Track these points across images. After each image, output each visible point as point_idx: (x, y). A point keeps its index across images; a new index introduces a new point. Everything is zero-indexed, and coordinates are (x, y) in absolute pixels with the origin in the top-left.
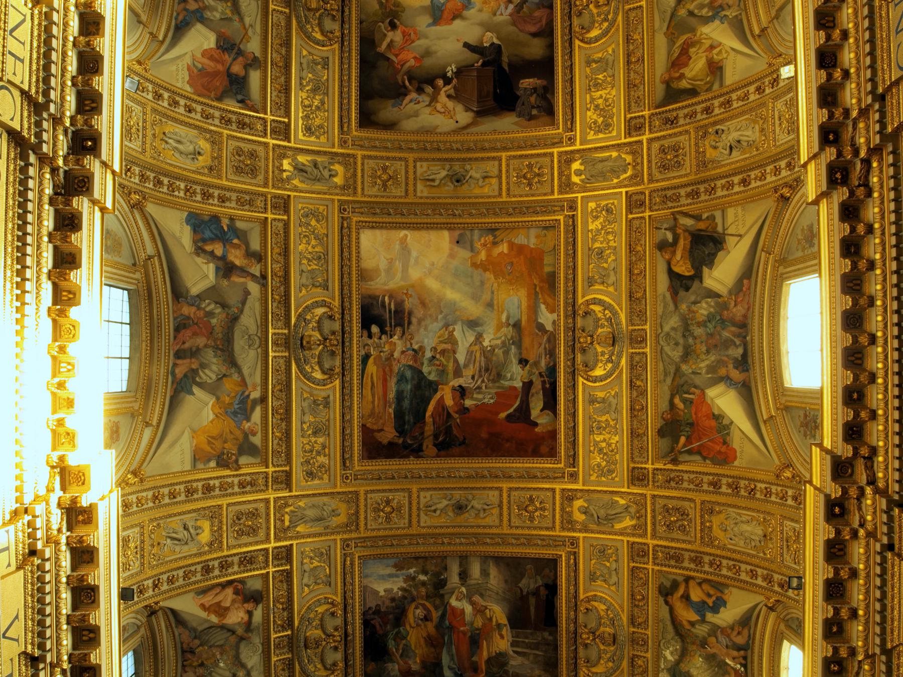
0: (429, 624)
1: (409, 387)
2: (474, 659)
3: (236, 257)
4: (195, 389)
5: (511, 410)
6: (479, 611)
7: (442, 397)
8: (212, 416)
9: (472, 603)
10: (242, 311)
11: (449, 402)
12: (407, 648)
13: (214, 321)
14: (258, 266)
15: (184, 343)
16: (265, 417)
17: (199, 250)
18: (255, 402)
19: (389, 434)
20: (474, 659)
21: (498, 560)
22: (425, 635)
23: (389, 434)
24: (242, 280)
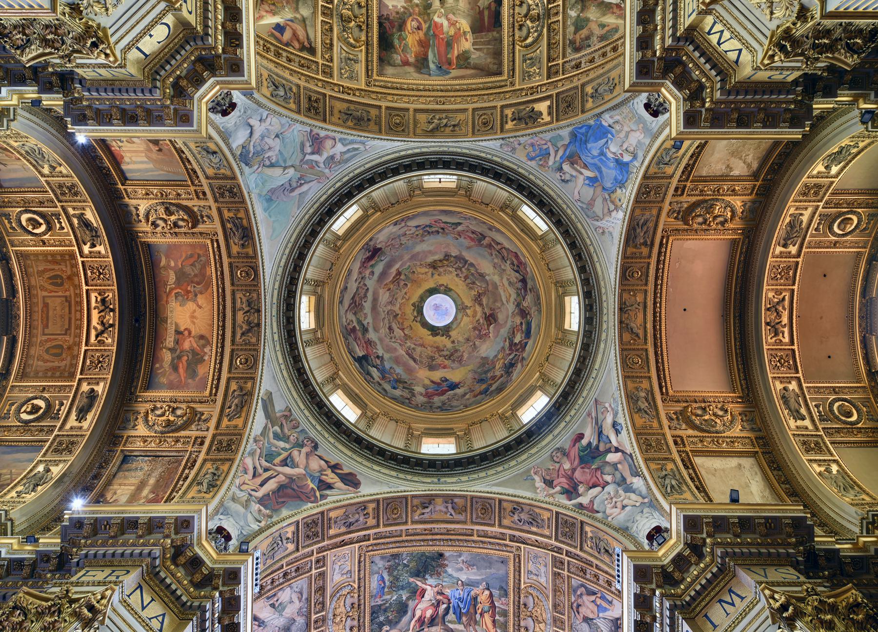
0: (420, 32)
2: (449, 56)
12: (406, 45)
20: (449, 56)
22: (418, 38)
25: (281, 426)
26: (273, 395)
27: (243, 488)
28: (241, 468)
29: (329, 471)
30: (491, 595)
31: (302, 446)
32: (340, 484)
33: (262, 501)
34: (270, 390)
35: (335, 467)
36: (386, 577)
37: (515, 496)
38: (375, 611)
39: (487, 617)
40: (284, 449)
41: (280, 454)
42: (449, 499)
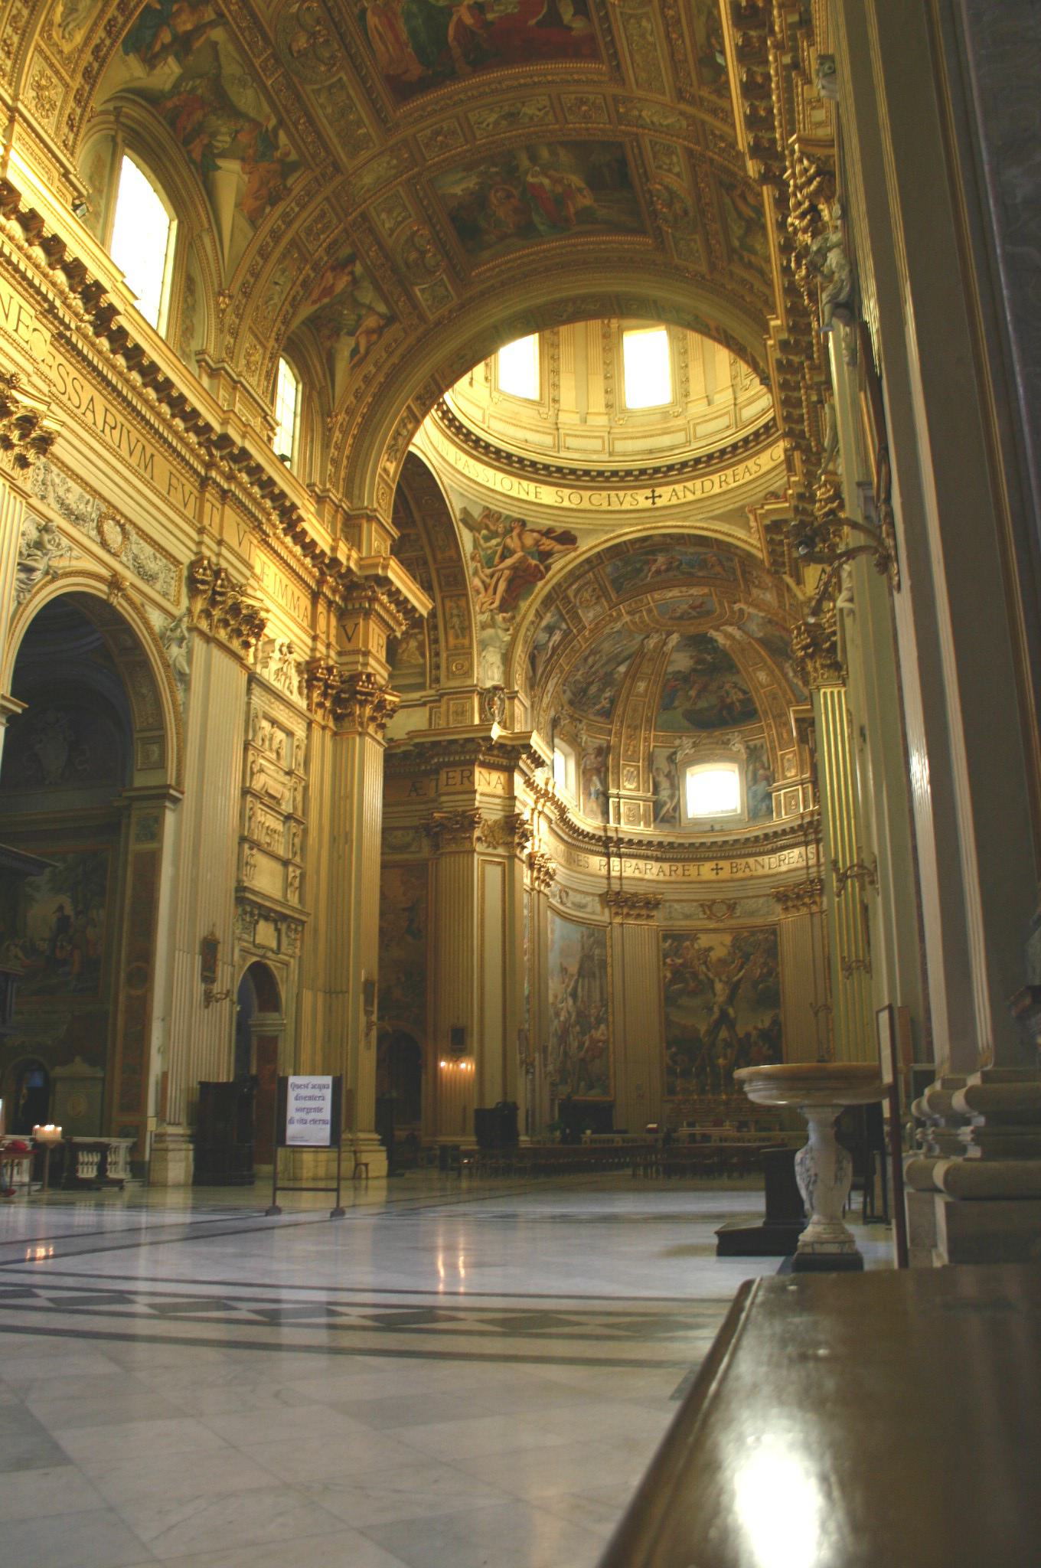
1: (420, 21)
3: (184, 23)
4: (220, 162)
5: (541, 16)
6: (555, 181)
7: (460, 20)
8: (246, 178)
9: (549, 177)
10: (220, 67)
11: (468, 20)
13: (199, 92)
14: (210, 8)
15: (185, 129)
16: (290, 135)
17: (151, 61)
18: (275, 131)
19: (416, 70)
21: (563, 144)
23: (416, 70)
24: (203, 39)
25: (487, 527)
26: (469, 509)
27: (483, 610)
28: (474, 593)
29: (544, 540)
30: (719, 560)
31: (512, 530)
32: (559, 547)
33: (502, 608)
34: (463, 506)
35: (548, 533)
36: (619, 563)
37: (729, 535)
38: (613, 582)
39: (718, 569)
40: (498, 545)
41: (495, 552)
42: (664, 535)
